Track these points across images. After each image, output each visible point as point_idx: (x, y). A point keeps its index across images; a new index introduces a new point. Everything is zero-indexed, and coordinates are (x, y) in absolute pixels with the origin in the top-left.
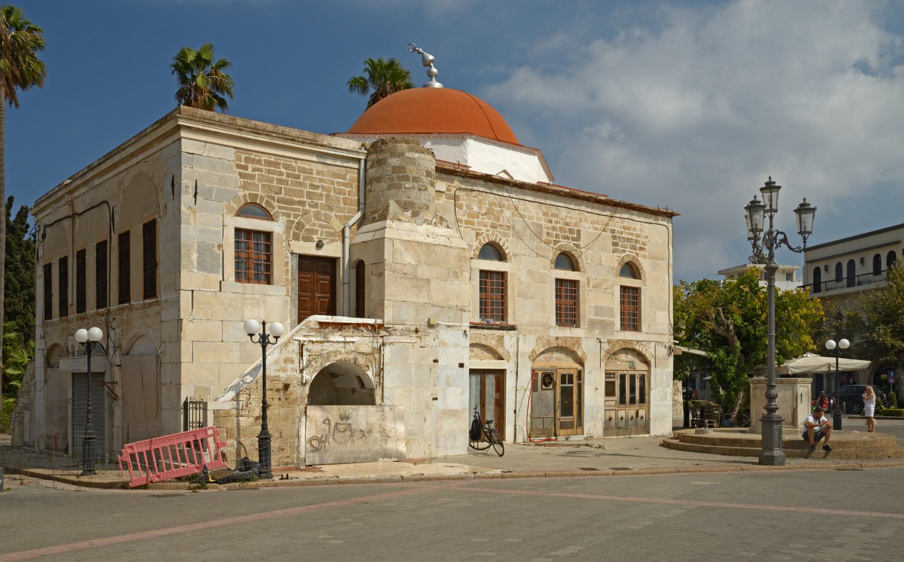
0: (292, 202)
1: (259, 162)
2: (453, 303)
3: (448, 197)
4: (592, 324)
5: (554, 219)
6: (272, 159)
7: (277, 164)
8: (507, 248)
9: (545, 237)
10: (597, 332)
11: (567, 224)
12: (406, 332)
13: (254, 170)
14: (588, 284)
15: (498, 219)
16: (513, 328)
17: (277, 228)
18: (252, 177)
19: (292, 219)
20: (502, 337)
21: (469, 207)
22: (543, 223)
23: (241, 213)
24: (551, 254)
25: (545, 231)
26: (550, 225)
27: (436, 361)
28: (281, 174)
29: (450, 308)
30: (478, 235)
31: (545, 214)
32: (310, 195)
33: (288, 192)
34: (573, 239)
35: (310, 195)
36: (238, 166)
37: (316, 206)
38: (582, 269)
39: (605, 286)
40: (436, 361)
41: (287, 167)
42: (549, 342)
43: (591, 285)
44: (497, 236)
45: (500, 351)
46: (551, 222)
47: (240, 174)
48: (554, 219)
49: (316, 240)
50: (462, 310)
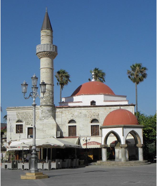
0: (27, 119)
1: (20, 113)
3: (60, 112)
5: (90, 112)
6: (23, 112)
7: (23, 113)
9: (87, 116)
11: (94, 113)
13: (19, 115)
15: (73, 115)
17: (23, 123)
19: (26, 122)
22: (87, 114)
23: (17, 122)
24: (90, 120)
25: (87, 115)
26: (89, 114)
28: (24, 114)
30: (68, 119)
31: (87, 112)
32: (30, 117)
34: (96, 116)
35: (30, 117)
36: (16, 115)
37: (31, 119)
41: (25, 113)
44: (73, 118)
46: (89, 113)
47: (17, 116)
48: (90, 112)
49: (31, 124)
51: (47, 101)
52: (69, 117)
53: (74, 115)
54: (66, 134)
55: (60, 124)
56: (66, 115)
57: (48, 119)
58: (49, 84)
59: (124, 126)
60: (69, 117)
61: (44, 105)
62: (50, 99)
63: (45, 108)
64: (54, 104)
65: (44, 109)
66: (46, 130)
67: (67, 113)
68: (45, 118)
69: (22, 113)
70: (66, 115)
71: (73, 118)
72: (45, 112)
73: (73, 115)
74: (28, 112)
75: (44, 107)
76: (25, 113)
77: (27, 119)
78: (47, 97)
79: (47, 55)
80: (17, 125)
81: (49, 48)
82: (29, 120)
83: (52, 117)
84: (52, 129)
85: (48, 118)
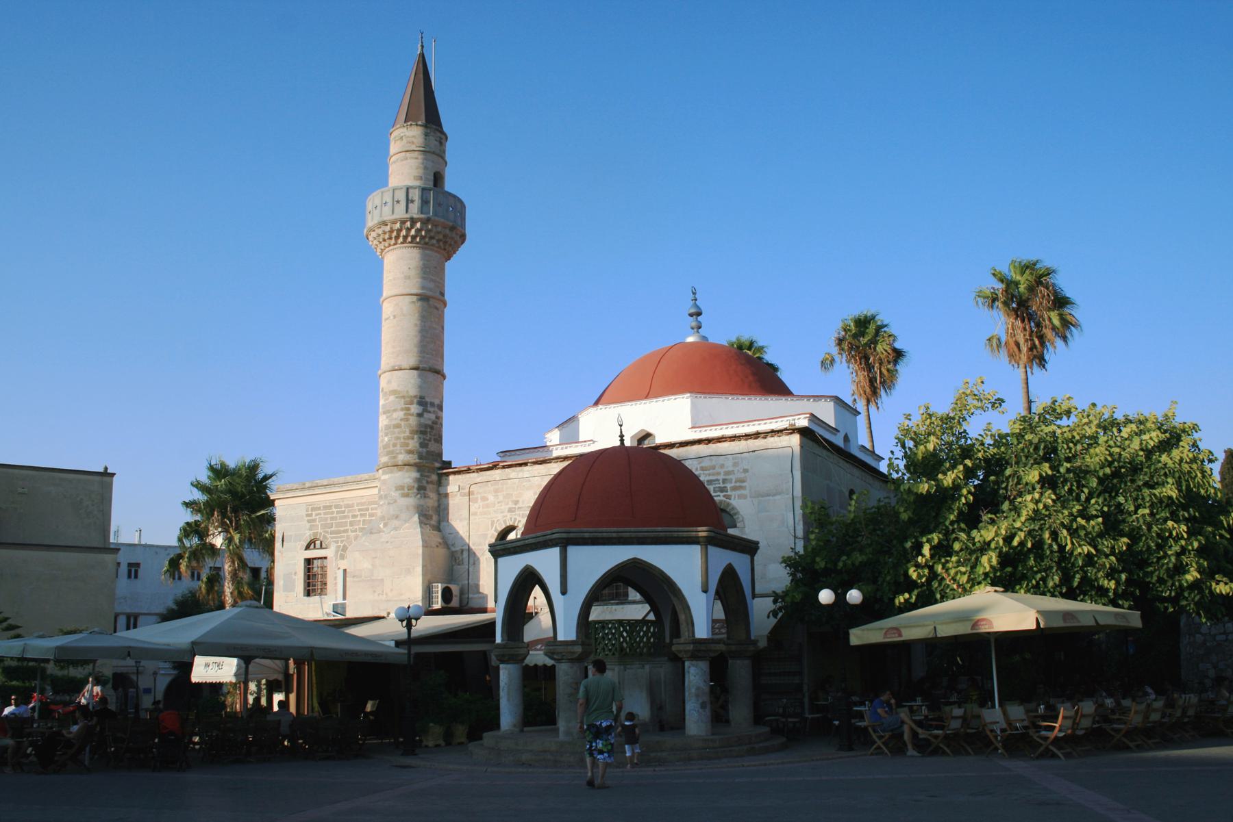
0: (339, 532)
7: (330, 507)
15: (516, 502)
17: (328, 553)
18: (314, 520)
21: (484, 499)
23: (308, 548)
30: (493, 523)
32: (352, 524)
33: (338, 525)
35: (352, 524)
41: (336, 507)
47: (309, 521)
51: (395, 445)
52: (500, 516)
53: (520, 505)
55: (462, 551)
56: (488, 506)
57: (396, 529)
58: (405, 365)
59: (564, 535)
60: (500, 516)
61: (386, 466)
62: (407, 434)
63: (386, 477)
64: (445, 458)
65: (384, 482)
66: (382, 580)
67: (491, 498)
68: (385, 525)
69: (325, 507)
70: (488, 506)
72: (386, 496)
73: (516, 502)
75: (384, 473)
76: (336, 507)
77: (339, 532)
78: (398, 426)
79: (397, 237)
80: (309, 562)
81: (403, 203)
82: (348, 537)
83: (416, 518)
84: (409, 571)
85: (396, 523)
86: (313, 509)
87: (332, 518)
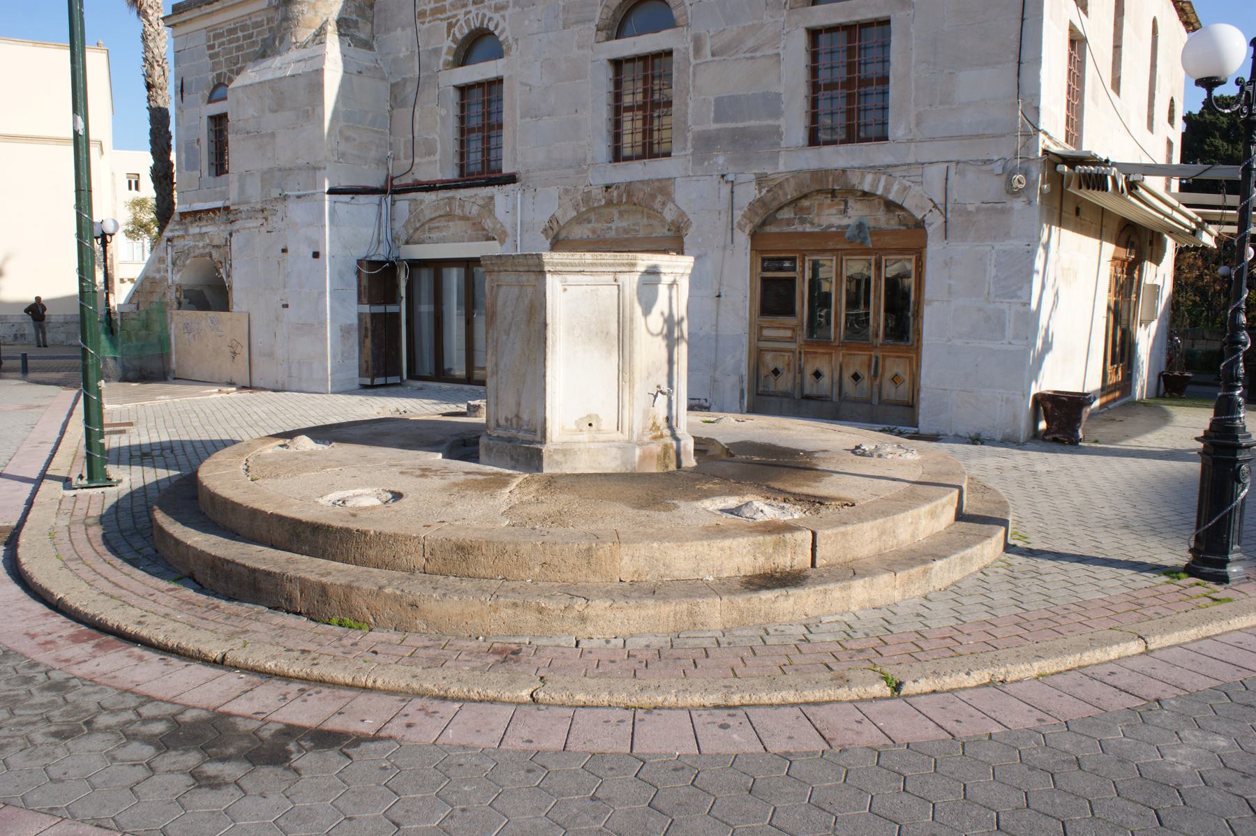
2: (300, 162)
4: (706, 144)
8: (502, 32)
10: (721, 160)
12: (252, 214)
14: (698, 50)
16: (512, 179)
20: (492, 198)
27: (284, 251)
28: (238, 39)
29: (300, 169)
30: (450, 26)
36: (211, 47)
38: (680, 21)
39: (750, 43)
40: (284, 251)
41: (243, 28)
42: (587, 197)
43: (707, 50)
45: (488, 224)
47: (211, 56)
50: (315, 169)
54: (438, 156)
66: (273, 135)
69: (232, 31)
71: (484, 15)
74: (254, 20)
76: (243, 28)
86: (216, 37)
87: (239, 49)
